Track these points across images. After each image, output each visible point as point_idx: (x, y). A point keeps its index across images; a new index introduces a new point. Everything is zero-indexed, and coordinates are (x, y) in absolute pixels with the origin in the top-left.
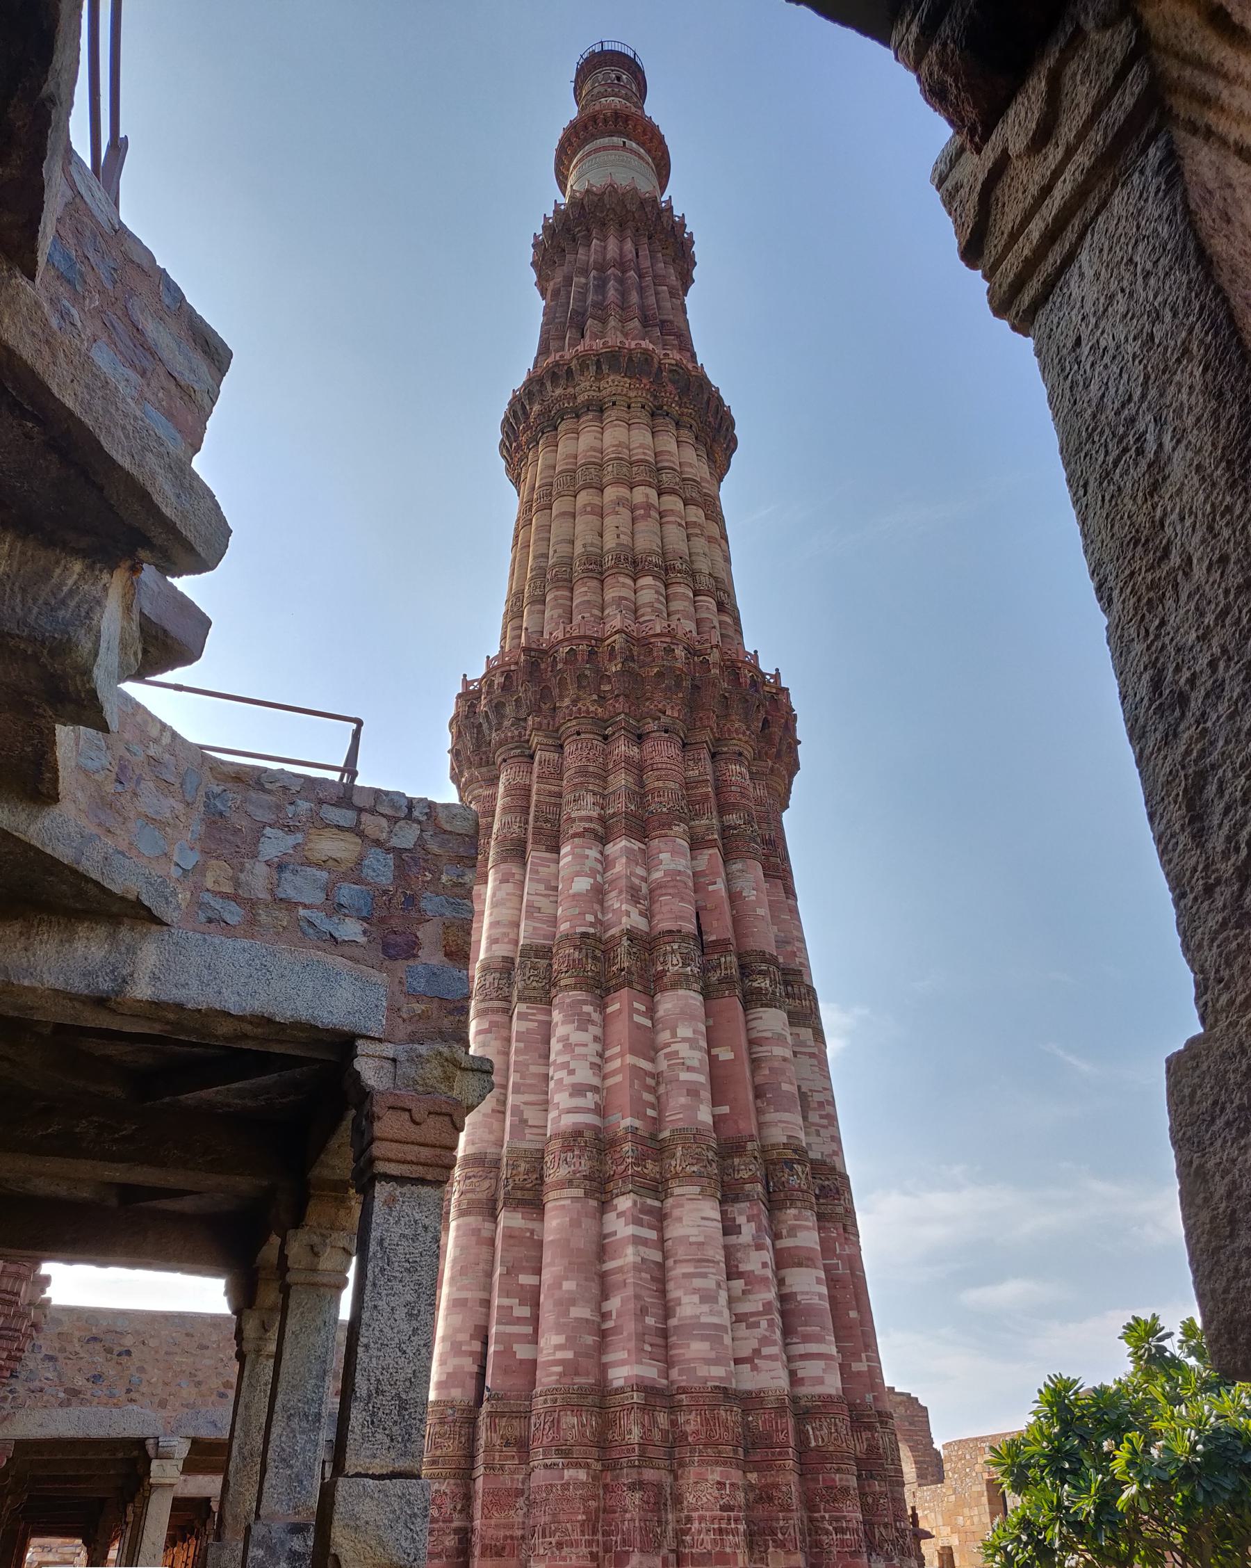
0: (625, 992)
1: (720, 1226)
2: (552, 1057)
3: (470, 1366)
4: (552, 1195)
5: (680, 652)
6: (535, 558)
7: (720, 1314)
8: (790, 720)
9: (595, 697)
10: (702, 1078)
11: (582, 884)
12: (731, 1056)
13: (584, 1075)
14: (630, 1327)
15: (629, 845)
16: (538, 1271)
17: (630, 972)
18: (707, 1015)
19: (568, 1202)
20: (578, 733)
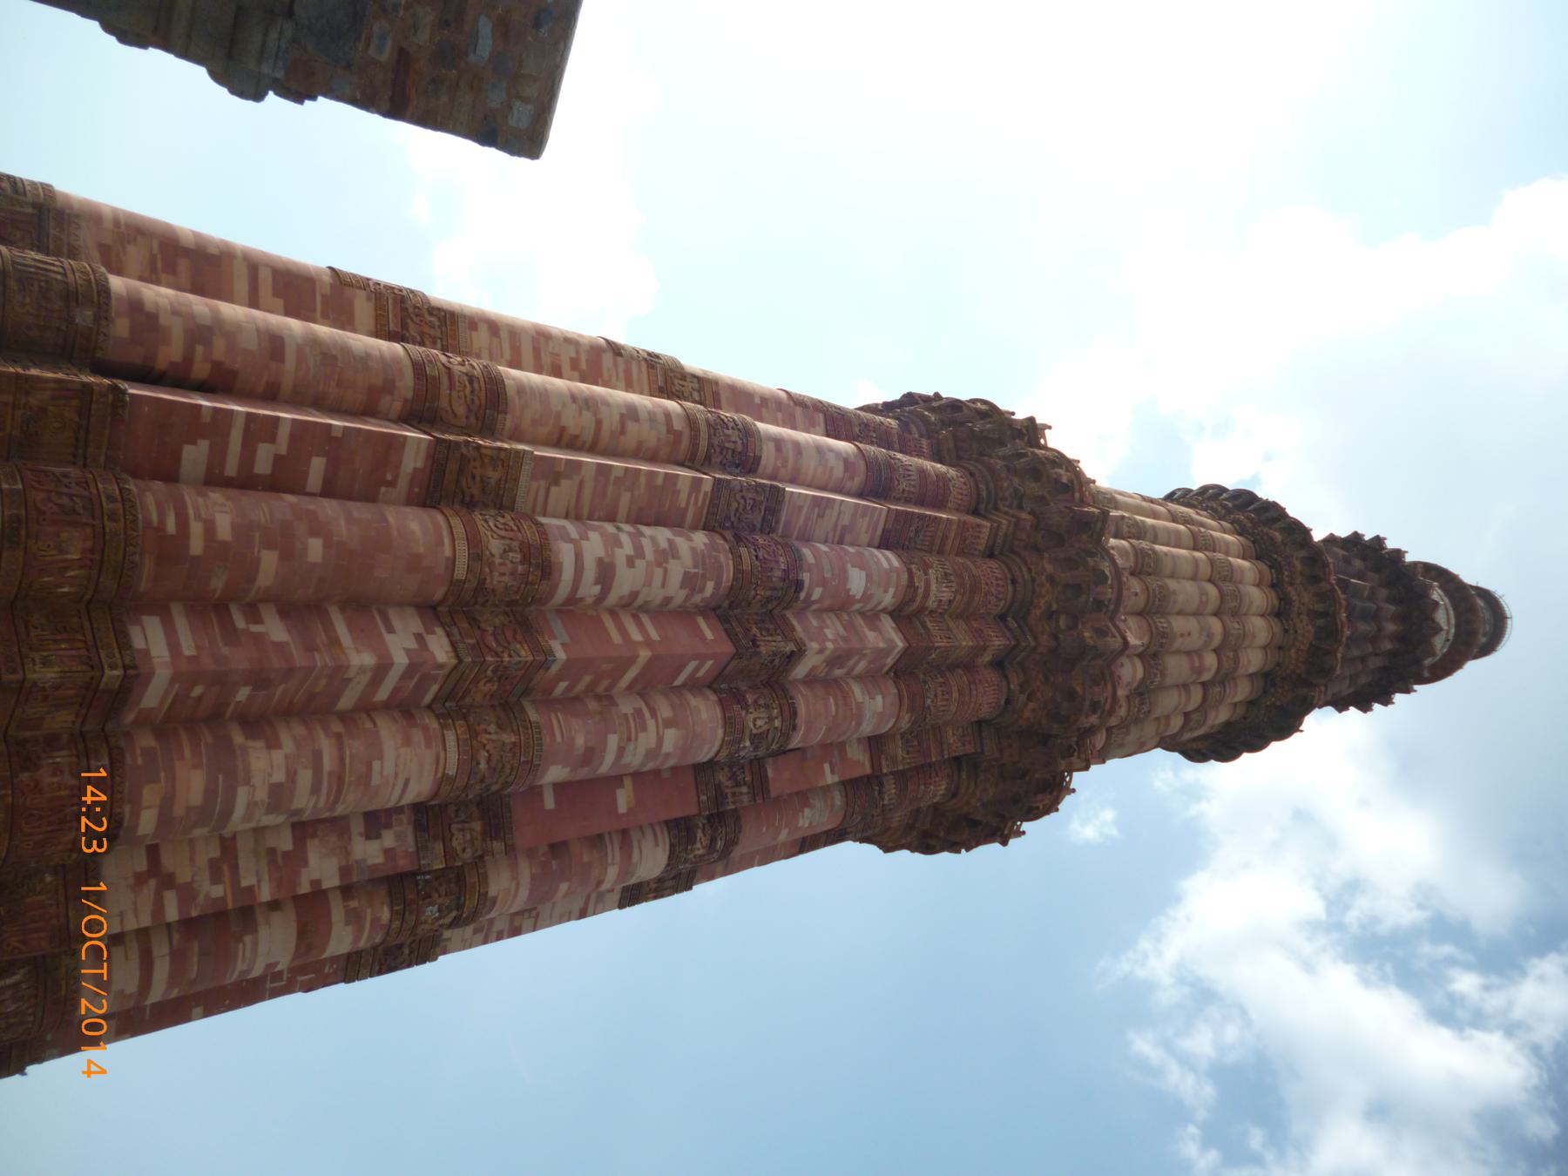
0: (728, 648)
2: (647, 530)
3: (171, 353)
4: (457, 523)
5: (1094, 719)
6: (1153, 527)
7: (248, 817)
9: (1055, 607)
10: (604, 769)
11: (857, 582)
12: (622, 808)
13: (626, 579)
14: (239, 659)
16: (328, 491)
19: (448, 552)
20: (1014, 581)
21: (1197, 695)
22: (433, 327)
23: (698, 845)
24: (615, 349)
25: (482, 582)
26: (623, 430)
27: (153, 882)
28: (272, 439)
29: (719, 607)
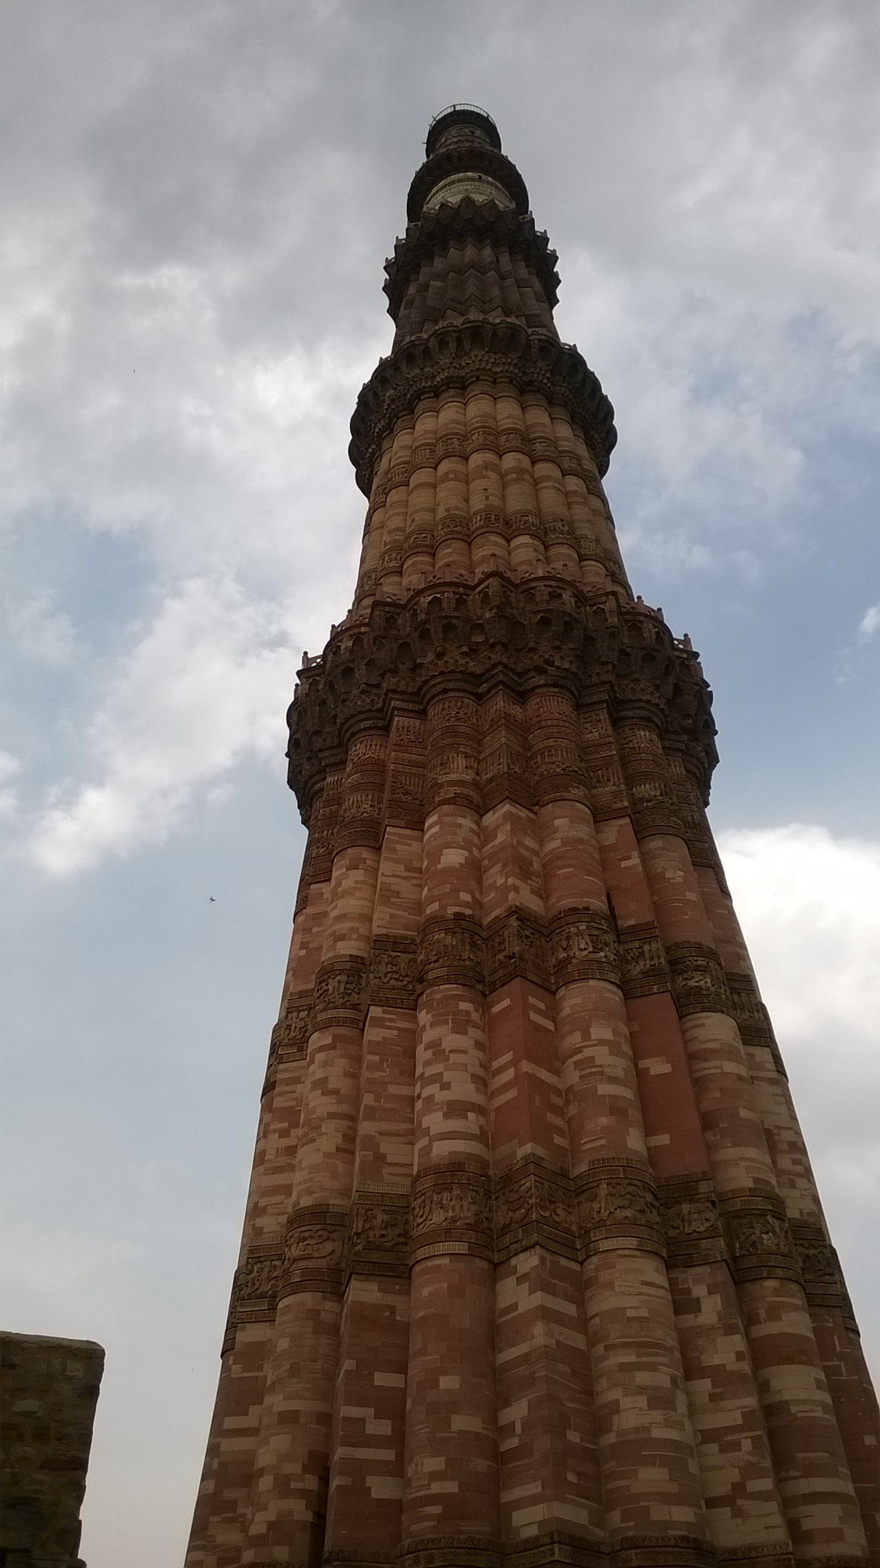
1: (669, 1297)
2: (419, 1070)
3: (299, 1510)
4: (421, 1254)
5: (566, 596)
6: (389, 532)
7: (680, 1426)
8: (703, 696)
11: (453, 857)
12: (667, 1068)
13: (463, 1089)
15: (514, 810)
16: (402, 1368)
17: (521, 958)
18: (629, 1019)
19: (445, 1261)
20: (445, 691)
21: (544, 469)
22: (261, 1270)
23: (702, 983)
24: (269, 1088)
25: (470, 1227)
26: (336, 1092)
27: (739, 1502)
28: (362, 1421)
29: (482, 993)
